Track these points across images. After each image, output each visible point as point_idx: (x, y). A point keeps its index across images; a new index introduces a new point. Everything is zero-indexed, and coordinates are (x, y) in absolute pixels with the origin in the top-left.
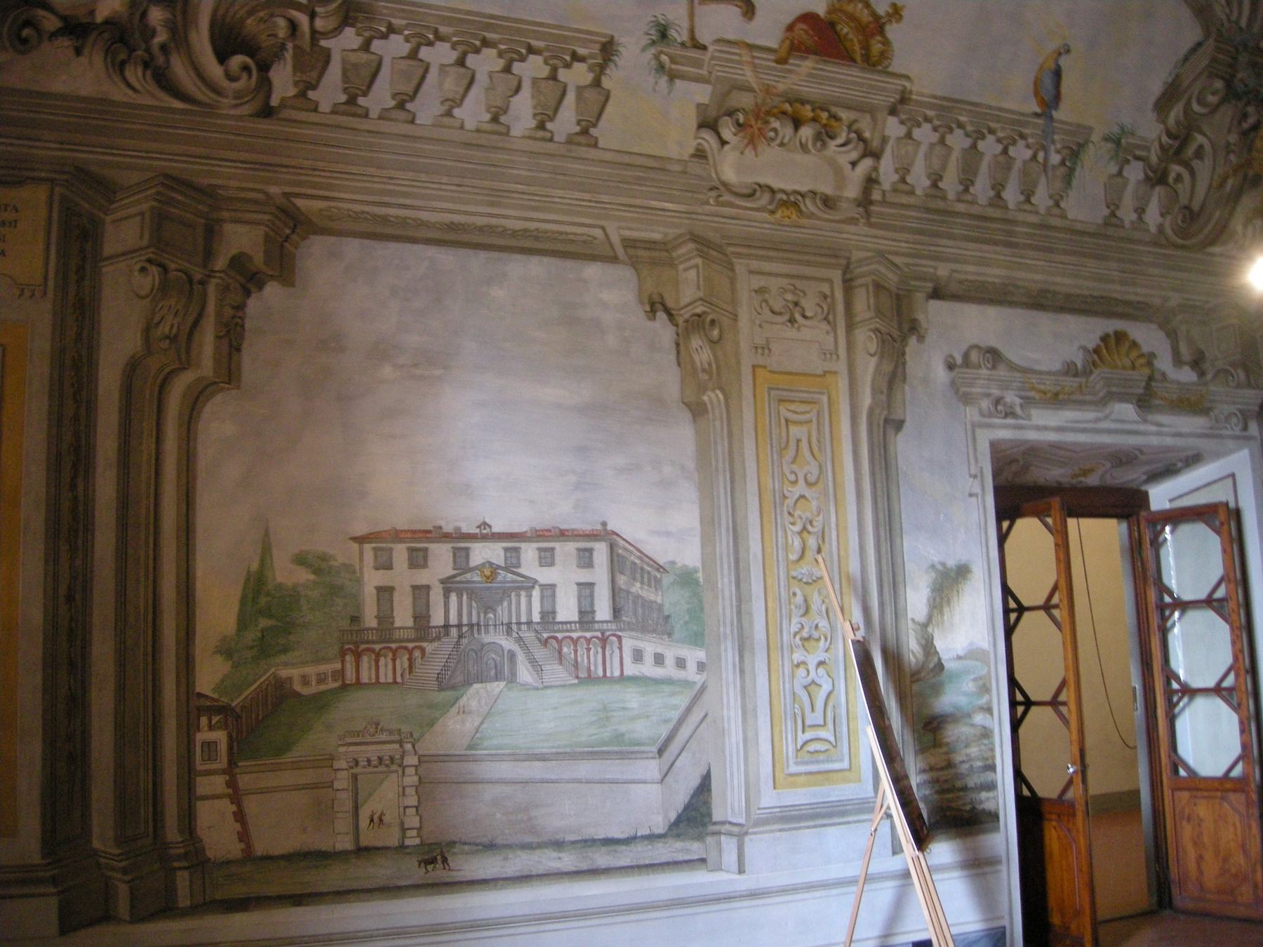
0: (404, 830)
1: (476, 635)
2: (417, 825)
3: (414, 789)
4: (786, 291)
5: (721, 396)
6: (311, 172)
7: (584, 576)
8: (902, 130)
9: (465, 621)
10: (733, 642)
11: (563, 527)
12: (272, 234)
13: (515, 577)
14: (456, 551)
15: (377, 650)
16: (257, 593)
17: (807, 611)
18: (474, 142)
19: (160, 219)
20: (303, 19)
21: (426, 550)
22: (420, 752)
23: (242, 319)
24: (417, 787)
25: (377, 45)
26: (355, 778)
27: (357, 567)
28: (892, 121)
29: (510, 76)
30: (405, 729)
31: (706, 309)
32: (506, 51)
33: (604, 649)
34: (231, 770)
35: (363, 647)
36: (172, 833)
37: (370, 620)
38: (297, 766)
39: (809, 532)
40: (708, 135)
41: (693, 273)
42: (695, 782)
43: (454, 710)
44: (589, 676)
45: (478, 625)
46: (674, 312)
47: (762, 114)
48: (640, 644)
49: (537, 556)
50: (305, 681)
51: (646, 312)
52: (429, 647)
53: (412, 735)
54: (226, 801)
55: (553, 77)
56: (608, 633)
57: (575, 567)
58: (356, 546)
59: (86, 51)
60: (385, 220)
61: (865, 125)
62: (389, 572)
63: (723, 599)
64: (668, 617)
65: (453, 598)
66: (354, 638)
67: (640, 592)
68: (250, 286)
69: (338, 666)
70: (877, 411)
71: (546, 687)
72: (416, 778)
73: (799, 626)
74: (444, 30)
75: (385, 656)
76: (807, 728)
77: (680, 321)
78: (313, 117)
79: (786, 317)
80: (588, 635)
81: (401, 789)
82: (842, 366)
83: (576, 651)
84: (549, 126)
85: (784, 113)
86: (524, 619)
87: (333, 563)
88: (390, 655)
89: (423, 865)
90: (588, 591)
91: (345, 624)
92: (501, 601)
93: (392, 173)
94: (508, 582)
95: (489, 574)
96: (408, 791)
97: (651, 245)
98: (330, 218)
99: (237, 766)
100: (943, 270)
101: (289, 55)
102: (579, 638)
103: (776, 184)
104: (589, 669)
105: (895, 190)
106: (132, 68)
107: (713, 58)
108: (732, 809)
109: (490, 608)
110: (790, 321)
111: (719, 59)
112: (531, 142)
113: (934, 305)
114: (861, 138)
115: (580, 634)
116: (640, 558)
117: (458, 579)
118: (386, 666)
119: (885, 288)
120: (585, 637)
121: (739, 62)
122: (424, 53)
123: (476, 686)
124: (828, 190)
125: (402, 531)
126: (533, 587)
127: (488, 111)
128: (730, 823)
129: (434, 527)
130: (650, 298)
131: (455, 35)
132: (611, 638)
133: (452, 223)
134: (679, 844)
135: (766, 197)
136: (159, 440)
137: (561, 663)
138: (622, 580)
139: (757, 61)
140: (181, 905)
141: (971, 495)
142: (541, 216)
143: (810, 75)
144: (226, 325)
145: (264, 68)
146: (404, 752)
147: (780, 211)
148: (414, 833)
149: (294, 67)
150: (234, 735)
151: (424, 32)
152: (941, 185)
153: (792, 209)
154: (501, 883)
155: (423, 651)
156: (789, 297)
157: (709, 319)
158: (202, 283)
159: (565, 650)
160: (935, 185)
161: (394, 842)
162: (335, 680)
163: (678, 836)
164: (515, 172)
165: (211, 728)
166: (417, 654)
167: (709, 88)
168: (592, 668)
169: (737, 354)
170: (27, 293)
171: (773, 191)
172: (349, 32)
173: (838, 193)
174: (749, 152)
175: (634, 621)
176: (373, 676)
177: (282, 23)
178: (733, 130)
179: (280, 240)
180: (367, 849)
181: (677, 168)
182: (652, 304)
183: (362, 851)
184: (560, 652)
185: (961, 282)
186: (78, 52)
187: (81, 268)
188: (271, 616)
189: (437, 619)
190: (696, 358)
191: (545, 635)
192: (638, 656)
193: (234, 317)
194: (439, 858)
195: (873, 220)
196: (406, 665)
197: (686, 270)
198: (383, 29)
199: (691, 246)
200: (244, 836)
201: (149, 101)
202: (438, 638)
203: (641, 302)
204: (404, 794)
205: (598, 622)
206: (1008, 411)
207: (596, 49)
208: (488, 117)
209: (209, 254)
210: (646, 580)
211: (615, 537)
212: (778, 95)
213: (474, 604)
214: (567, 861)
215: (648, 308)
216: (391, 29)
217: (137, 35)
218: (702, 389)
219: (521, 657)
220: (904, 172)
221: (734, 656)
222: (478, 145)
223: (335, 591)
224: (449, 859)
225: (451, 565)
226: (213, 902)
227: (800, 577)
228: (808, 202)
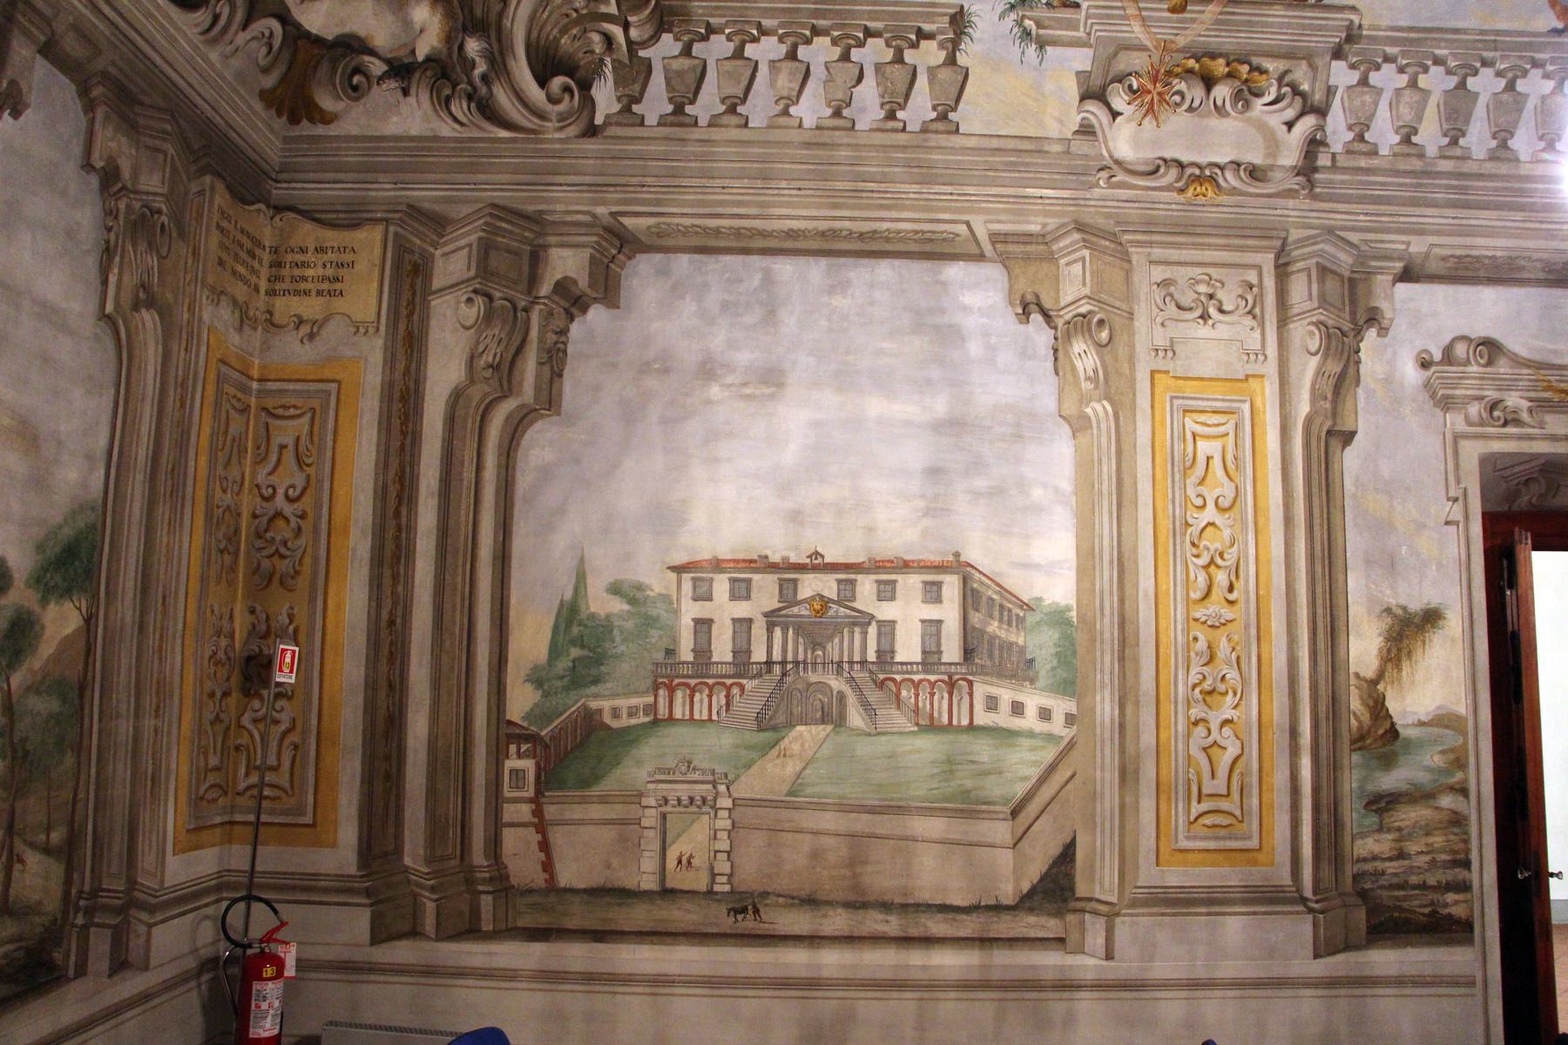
0: (713, 875)
2: (728, 871)
4: (1198, 282)
5: (1109, 408)
6: (639, 189)
7: (932, 612)
8: (1355, 76)
9: (790, 657)
10: (1112, 693)
11: (907, 558)
12: (597, 255)
14: (782, 582)
16: (569, 623)
17: (1211, 659)
18: (814, 141)
19: (486, 248)
20: (617, 31)
21: (749, 581)
23: (565, 344)
24: (729, 832)
25: (697, 48)
26: (664, 816)
27: (675, 598)
28: (1339, 66)
29: (851, 65)
30: (719, 769)
31: (1091, 308)
32: (840, 38)
33: (951, 694)
34: (537, 801)
35: (677, 681)
36: (478, 857)
37: (686, 654)
38: (604, 800)
39: (1218, 567)
40: (1093, 106)
41: (1078, 268)
42: (1055, 850)
43: (774, 752)
45: (805, 662)
46: (1051, 313)
47: (1159, 76)
48: (994, 691)
49: (875, 590)
50: (616, 713)
51: (1017, 314)
52: (749, 684)
54: (532, 830)
55: (899, 59)
56: (957, 677)
57: (919, 601)
58: (674, 576)
59: (413, 91)
60: (717, 232)
61: (1301, 74)
62: (708, 603)
63: (1102, 642)
64: (1032, 661)
65: (778, 632)
67: (998, 632)
68: (574, 310)
69: (650, 699)
70: (1318, 421)
71: (878, 734)
72: (729, 822)
73: (1201, 677)
74: (767, 23)
76: (1204, 798)
77: (1060, 323)
78: (639, 132)
79: (1199, 312)
80: (933, 678)
82: (1271, 368)
83: (917, 696)
84: (900, 114)
85: (1190, 71)
86: (857, 658)
87: (649, 593)
88: (707, 691)
90: (934, 629)
91: (659, 656)
92: (831, 638)
93: (726, 183)
96: (719, 834)
97: (1026, 238)
98: (659, 235)
100: (1418, 246)
101: (608, 70)
102: (921, 681)
103: (1185, 159)
104: (931, 716)
105: (1349, 152)
106: (457, 102)
107: (1087, 18)
108: (1102, 887)
110: (1201, 317)
111: (1096, 16)
112: (880, 135)
113: (1402, 288)
114: (1296, 92)
115: (921, 677)
117: (783, 612)
118: (701, 701)
119: (1333, 272)
121: (1126, 17)
122: (750, 50)
123: (799, 728)
124: (1257, 158)
125: (724, 561)
126: (869, 623)
127: (829, 106)
128: (1098, 901)
130: (1023, 296)
131: (782, 25)
133: (792, 230)
134: (1032, 919)
135: (1173, 172)
136: (479, 468)
137: (898, 708)
138: (976, 618)
139: (1144, 13)
140: (484, 929)
141: (1447, 523)
142: (894, 214)
143: (1218, 22)
144: (549, 351)
145: (585, 86)
146: (717, 793)
147: (1191, 190)
148: (724, 879)
149: (615, 83)
151: (747, 28)
152: (1414, 139)
153: (1207, 185)
155: (742, 688)
156: (1202, 288)
157: (1095, 320)
158: (526, 310)
159: (904, 693)
160: (1407, 140)
161: (702, 885)
162: (646, 714)
163: (1031, 910)
164: (862, 169)
165: (519, 756)
166: (735, 690)
167: (1089, 52)
168: (936, 715)
169: (1132, 360)
170: (362, 330)
171: (1181, 166)
172: (667, 38)
173: (1269, 161)
174: (1148, 122)
176: (687, 712)
177: (596, 37)
178: (1126, 98)
179: (606, 261)
180: (673, 891)
181: (1056, 148)
182: (1025, 306)
183: (667, 893)
184: (898, 696)
185: (1444, 259)
186: (406, 92)
187: (411, 303)
188: (583, 647)
189: (759, 655)
190: (1079, 365)
191: (881, 677)
192: (992, 704)
193: (556, 343)
194: (750, 908)
195: (1318, 190)
196: (723, 701)
197: (1067, 264)
198: (703, 31)
199: (1077, 236)
200: (548, 866)
201: (476, 134)
202: (759, 675)
203: (1012, 304)
204: (715, 838)
205: (945, 664)
206: (1509, 417)
207: (944, 22)
208: (829, 112)
209: (533, 281)
210: (1006, 618)
211: (969, 569)
212: (1178, 51)
213: (801, 640)
214: (892, 925)
215: (1020, 311)
216: (711, 30)
217: (458, 69)
218: (1084, 400)
219: (851, 699)
220: (1360, 130)
221: (1112, 709)
222: (818, 144)
223: (650, 621)
224: (761, 909)
225: (777, 598)
226: (516, 928)
227: (1203, 619)
228: (1229, 175)
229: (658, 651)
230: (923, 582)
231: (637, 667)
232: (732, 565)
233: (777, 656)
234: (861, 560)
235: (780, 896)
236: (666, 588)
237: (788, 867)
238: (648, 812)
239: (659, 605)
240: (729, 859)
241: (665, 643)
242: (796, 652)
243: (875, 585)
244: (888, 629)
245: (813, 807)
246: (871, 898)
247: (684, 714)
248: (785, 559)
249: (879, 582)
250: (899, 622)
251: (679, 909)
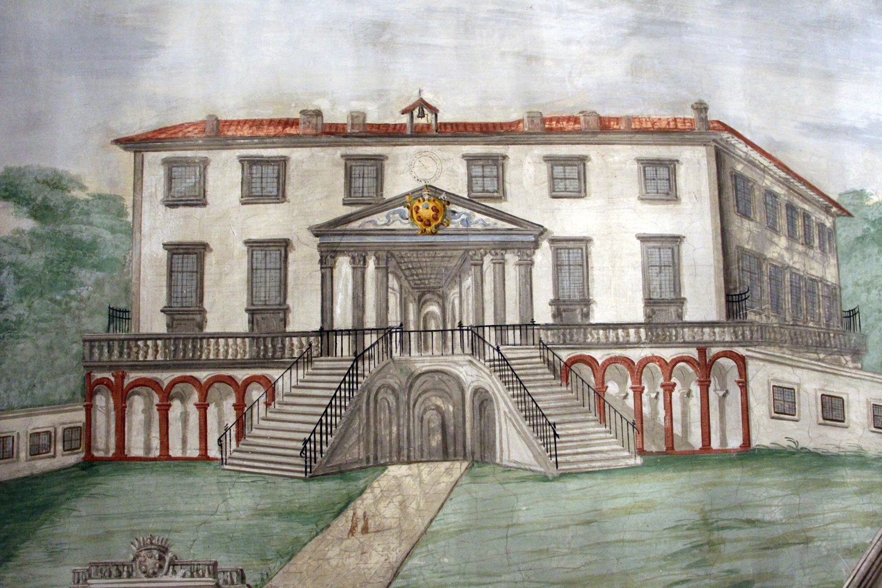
1: (396, 354)
9: (370, 321)
11: (605, 112)
13: (491, 221)
15: (166, 383)
21: (283, 162)
27: (129, 202)
30: (226, 562)
33: (705, 385)
35: (133, 376)
43: (342, 524)
44: (671, 448)
45: (402, 329)
48: (787, 376)
49: (544, 175)
53: (242, 578)
56: (714, 350)
57: (634, 201)
58: (128, 157)
62: (198, 211)
64: (853, 314)
65: (344, 267)
66: (115, 358)
67: (787, 256)
69: (78, 417)
71: (564, 475)
75: (183, 399)
80: (668, 354)
83: (638, 392)
86: (512, 318)
87: (76, 193)
88: (195, 397)
90: (666, 255)
91: (97, 325)
92: (457, 277)
94: (477, 232)
95: (426, 213)
102: (645, 362)
104: (669, 432)
109: (432, 290)
115: (647, 352)
116: (784, 183)
117: (355, 225)
120: (660, 360)
123: (395, 471)
125: (230, 123)
126: (536, 245)
129: (303, 112)
132: (723, 361)
137: (602, 420)
155: (270, 387)
159: (612, 388)
162: (69, 449)
166: (256, 393)
168: (677, 430)
175: (774, 320)
176: (156, 443)
184: (600, 393)
191: (565, 355)
196: (231, 418)
202: (306, 359)
205: (692, 325)
210: (800, 231)
211: (725, 135)
213: (393, 283)
225: (341, 195)
229: (92, 315)
230: (639, 160)
231: (50, 348)
232: (246, 131)
233: (343, 317)
234: (513, 117)
236: (112, 183)
239: (96, 218)
241: (110, 296)
242: (383, 308)
243: (544, 167)
244: (575, 256)
247: (148, 448)
248: (357, 117)
249: (552, 161)
250: (596, 242)
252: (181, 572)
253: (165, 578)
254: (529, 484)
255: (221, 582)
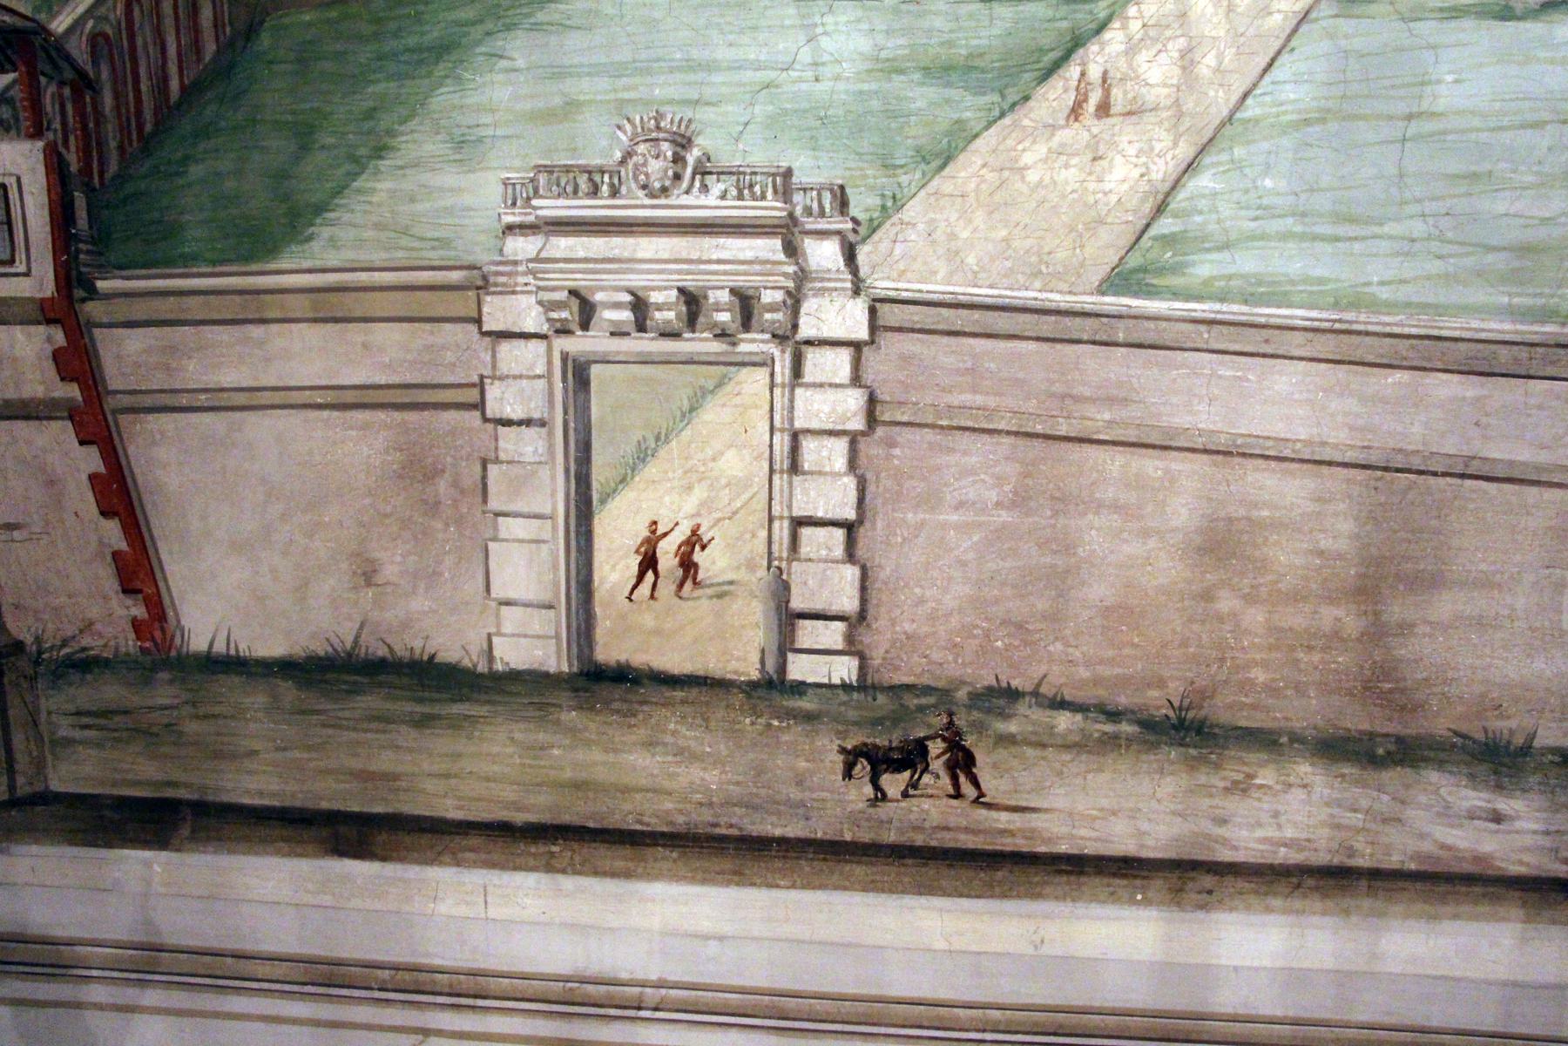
0: (788, 619)
2: (848, 602)
3: (840, 446)
22: (882, 284)
24: (854, 439)
26: (578, 374)
30: (811, 169)
43: (1056, 95)
53: (843, 204)
54: (62, 431)
72: (854, 400)
81: (782, 443)
89: (862, 767)
96: (809, 446)
99: (93, 293)
146: (802, 276)
148: (832, 634)
150: (73, 160)
154: (1208, 881)
180: (623, 677)
194: (935, 747)
204: (795, 467)
224: (980, 757)
226: (45, 798)
235: (1060, 704)
237: (1099, 591)
238: (515, 356)
240: (851, 556)
245: (1205, 335)
246: (1440, 725)
251: (650, 744)
252: (717, 188)
253: (686, 200)
254: (1468, 23)
255: (798, 211)
